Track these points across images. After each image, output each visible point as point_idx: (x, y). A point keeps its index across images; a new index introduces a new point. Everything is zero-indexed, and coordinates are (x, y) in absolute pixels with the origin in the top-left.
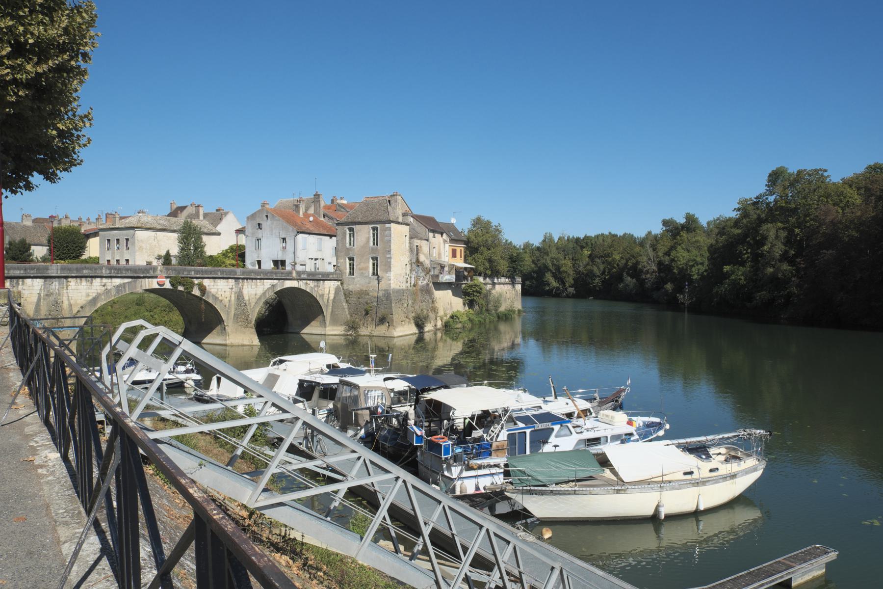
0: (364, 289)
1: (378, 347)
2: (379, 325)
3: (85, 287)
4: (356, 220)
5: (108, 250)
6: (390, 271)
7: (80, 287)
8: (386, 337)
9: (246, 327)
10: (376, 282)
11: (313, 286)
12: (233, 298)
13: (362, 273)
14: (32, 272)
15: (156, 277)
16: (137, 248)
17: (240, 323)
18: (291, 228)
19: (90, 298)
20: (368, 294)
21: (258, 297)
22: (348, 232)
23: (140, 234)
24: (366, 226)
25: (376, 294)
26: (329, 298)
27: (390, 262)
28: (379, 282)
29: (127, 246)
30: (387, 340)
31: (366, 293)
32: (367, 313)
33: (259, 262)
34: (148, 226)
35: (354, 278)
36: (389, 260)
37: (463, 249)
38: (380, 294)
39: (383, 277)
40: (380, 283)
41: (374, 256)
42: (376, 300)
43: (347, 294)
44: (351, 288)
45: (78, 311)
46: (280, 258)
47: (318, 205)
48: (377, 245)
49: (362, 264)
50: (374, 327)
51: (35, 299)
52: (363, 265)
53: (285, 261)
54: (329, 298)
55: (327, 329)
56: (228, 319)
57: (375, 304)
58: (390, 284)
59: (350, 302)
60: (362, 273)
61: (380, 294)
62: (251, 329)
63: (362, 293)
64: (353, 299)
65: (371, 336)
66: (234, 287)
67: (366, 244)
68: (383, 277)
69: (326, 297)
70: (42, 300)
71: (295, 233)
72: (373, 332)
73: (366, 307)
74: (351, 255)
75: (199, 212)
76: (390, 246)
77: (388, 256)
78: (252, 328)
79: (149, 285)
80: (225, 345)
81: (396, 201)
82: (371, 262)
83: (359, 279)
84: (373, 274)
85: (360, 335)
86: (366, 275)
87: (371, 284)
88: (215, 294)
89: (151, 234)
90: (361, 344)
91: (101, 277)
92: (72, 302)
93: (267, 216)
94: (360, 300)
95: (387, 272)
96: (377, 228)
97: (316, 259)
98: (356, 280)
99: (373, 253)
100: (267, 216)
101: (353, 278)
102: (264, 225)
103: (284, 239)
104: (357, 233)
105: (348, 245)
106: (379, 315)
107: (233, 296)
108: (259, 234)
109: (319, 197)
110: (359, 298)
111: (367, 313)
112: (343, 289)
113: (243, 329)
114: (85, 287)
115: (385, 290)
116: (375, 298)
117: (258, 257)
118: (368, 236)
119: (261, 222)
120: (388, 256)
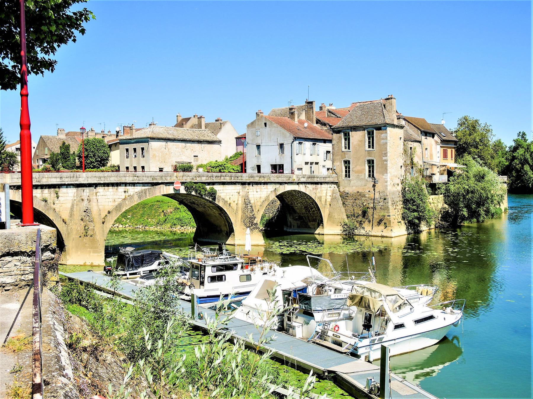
3: (112, 193)
5: (127, 158)
6: (387, 173)
7: (108, 193)
11: (311, 189)
12: (240, 202)
13: (358, 175)
14: (67, 180)
15: (172, 183)
16: (151, 156)
18: (288, 134)
19: (116, 203)
21: (262, 200)
23: (154, 144)
26: (326, 200)
27: (387, 164)
29: (142, 154)
33: (259, 167)
34: (161, 136)
36: (385, 163)
37: (453, 150)
43: (344, 196)
44: (348, 190)
45: (106, 216)
46: (278, 163)
47: (311, 112)
49: (358, 166)
51: (69, 205)
52: (358, 168)
53: (283, 165)
54: (326, 200)
55: (325, 229)
56: (236, 221)
58: (387, 186)
60: (358, 175)
63: (360, 195)
66: (241, 191)
69: (323, 200)
70: (75, 206)
74: (347, 159)
75: (201, 122)
76: (386, 148)
77: (384, 158)
79: (166, 192)
80: (234, 245)
81: (391, 104)
83: (355, 181)
84: (369, 176)
86: (363, 177)
88: (223, 197)
89: (163, 143)
91: (126, 184)
92: (100, 207)
93: (265, 124)
95: (383, 175)
97: (312, 163)
100: (265, 124)
103: (281, 146)
105: (343, 149)
107: (240, 199)
112: (339, 191)
114: (112, 193)
120: (384, 158)
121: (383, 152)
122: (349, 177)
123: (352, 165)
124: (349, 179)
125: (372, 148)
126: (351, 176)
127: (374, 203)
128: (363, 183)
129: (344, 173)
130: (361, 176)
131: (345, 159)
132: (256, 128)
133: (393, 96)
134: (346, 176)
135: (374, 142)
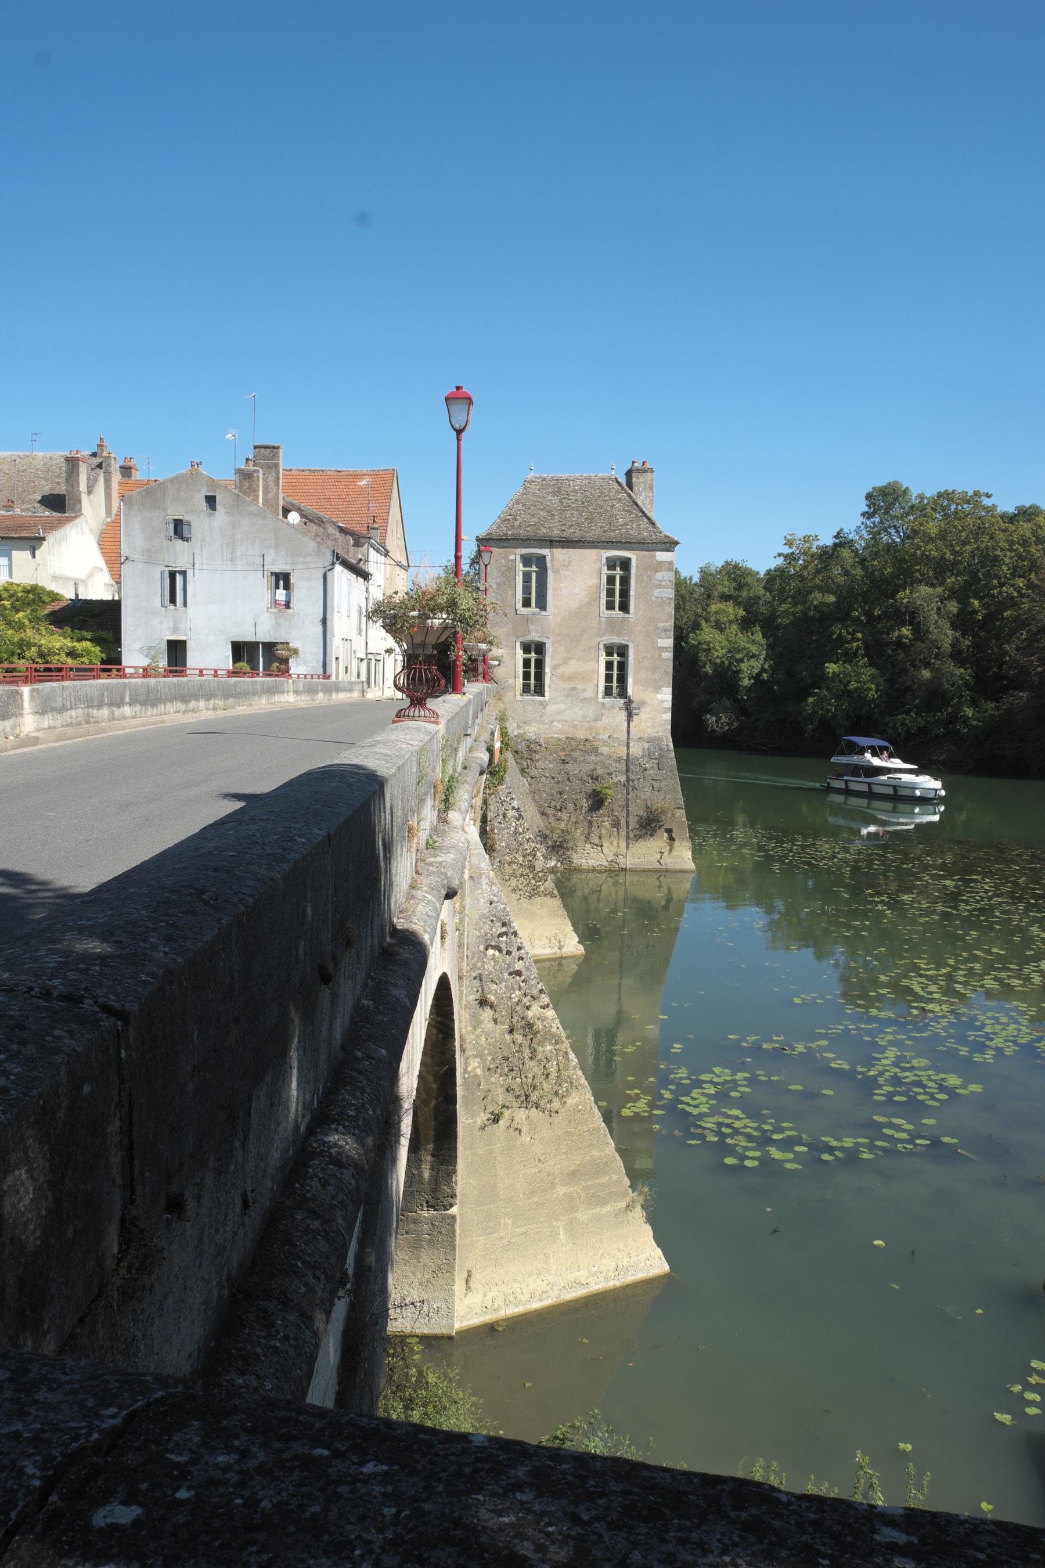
0: (581, 735)
1: (636, 901)
2: (638, 837)
4: (543, 532)
8: (667, 871)
9: (534, 893)
10: (623, 715)
13: (574, 689)
17: (513, 882)
20: (595, 751)
22: (520, 567)
24: (591, 554)
25: (622, 751)
28: (630, 715)
30: (666, 881)
31: (588, 747)
32: (597, 801)
35: (543, 705)
38: (636, 750)
39: (643, 703)
40: (635, 720)
41: (616, 640)
42: (623, 766)
44: (532, 731)
46: (264, 634)
48: (624, 607)
49: (572, 662)
50: (623, 844)
52: (574, 666)
57: (623, 778)
59: (534, 772)
60: (574, 689)
61: (636, 750)
62: (548, 900)
64: (546, 765)
65: (615, 872)
67: (589, 604)
68: (643, 703)
71: (329, 558)
72: (621, 860)
73: (590, 787)
74: (535, 636)
78: (552, 896)
81: (651, 488)
82: (603, 659)
83: (562, 706)
84: (608, 692)
85: (579, 870)
86: (589, 694)
87: (605, 721)
90: (579, 893)
93: (211, 500)
94: (569, 767)
96: (625, 564)
98: (551, 708)
99: (612, 632)
100: (211, 500)
101: (541, 703)
102: (201, 523)
103: (283, 579)
104: (556, 571)
105: (519, 605)
106: (637, 810)
108: (180, 555)
109: (276, 456)
110: (564, 762)
111: (597, 801)
113: (524, 902)
115: (650, 740)
116: (619, 760)
117: (175, 630)
118: (595, 581)
119: (186, 518)
121: (660, 625)
122: (540, 691)
123: (552, 657)
124: (541, 698)
125: (620, 609)
126: (547, 689)
127: (628, 770)
128: (590, 711)
129: (520, 681)
130: (584, 690)
131: (527, 638)
132: (165, 509)
133: (648, 466)
134: (526, 689)
135: (632, 593)
